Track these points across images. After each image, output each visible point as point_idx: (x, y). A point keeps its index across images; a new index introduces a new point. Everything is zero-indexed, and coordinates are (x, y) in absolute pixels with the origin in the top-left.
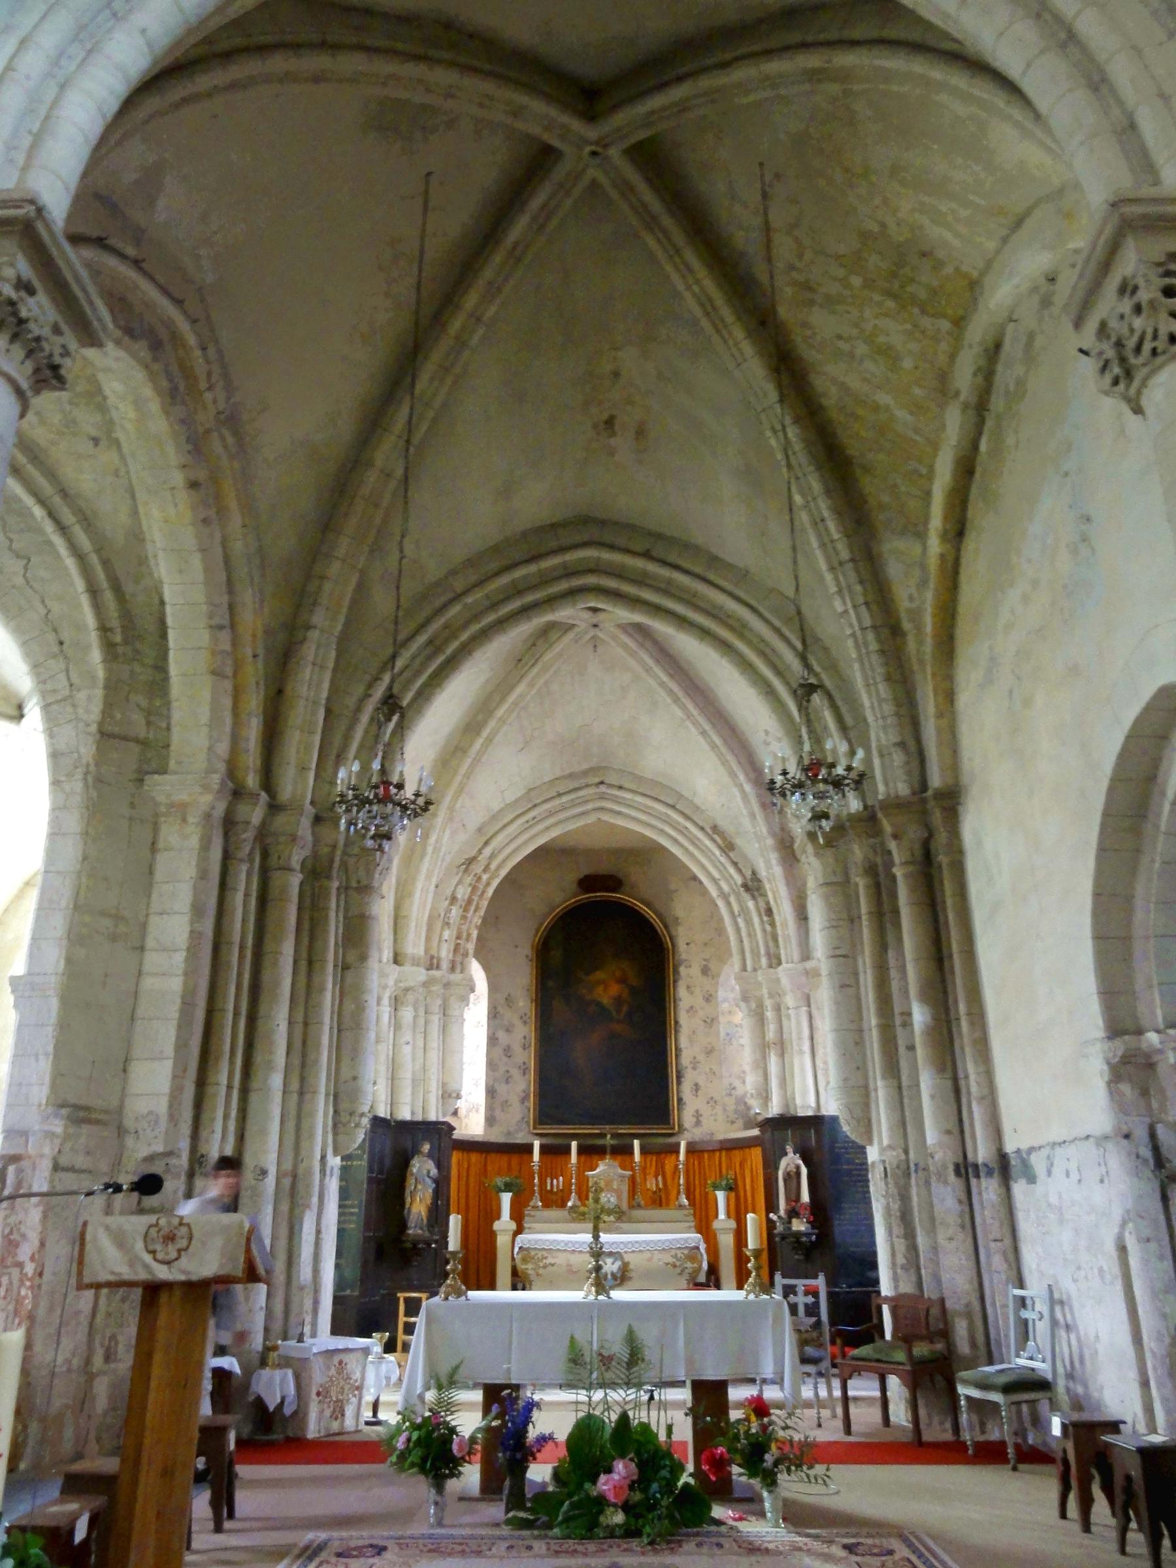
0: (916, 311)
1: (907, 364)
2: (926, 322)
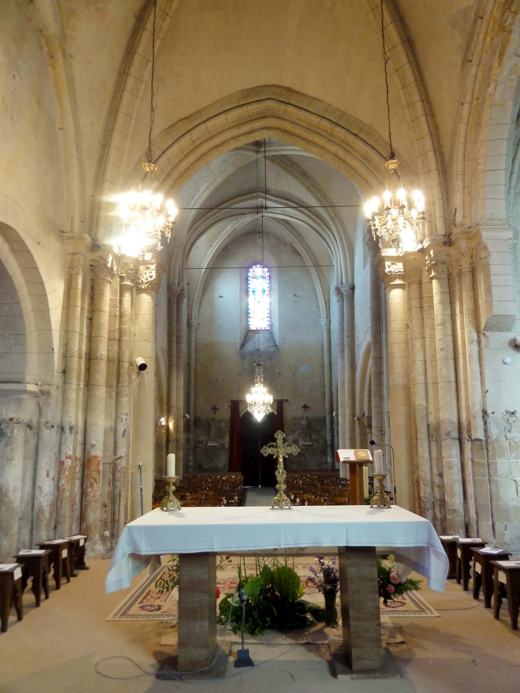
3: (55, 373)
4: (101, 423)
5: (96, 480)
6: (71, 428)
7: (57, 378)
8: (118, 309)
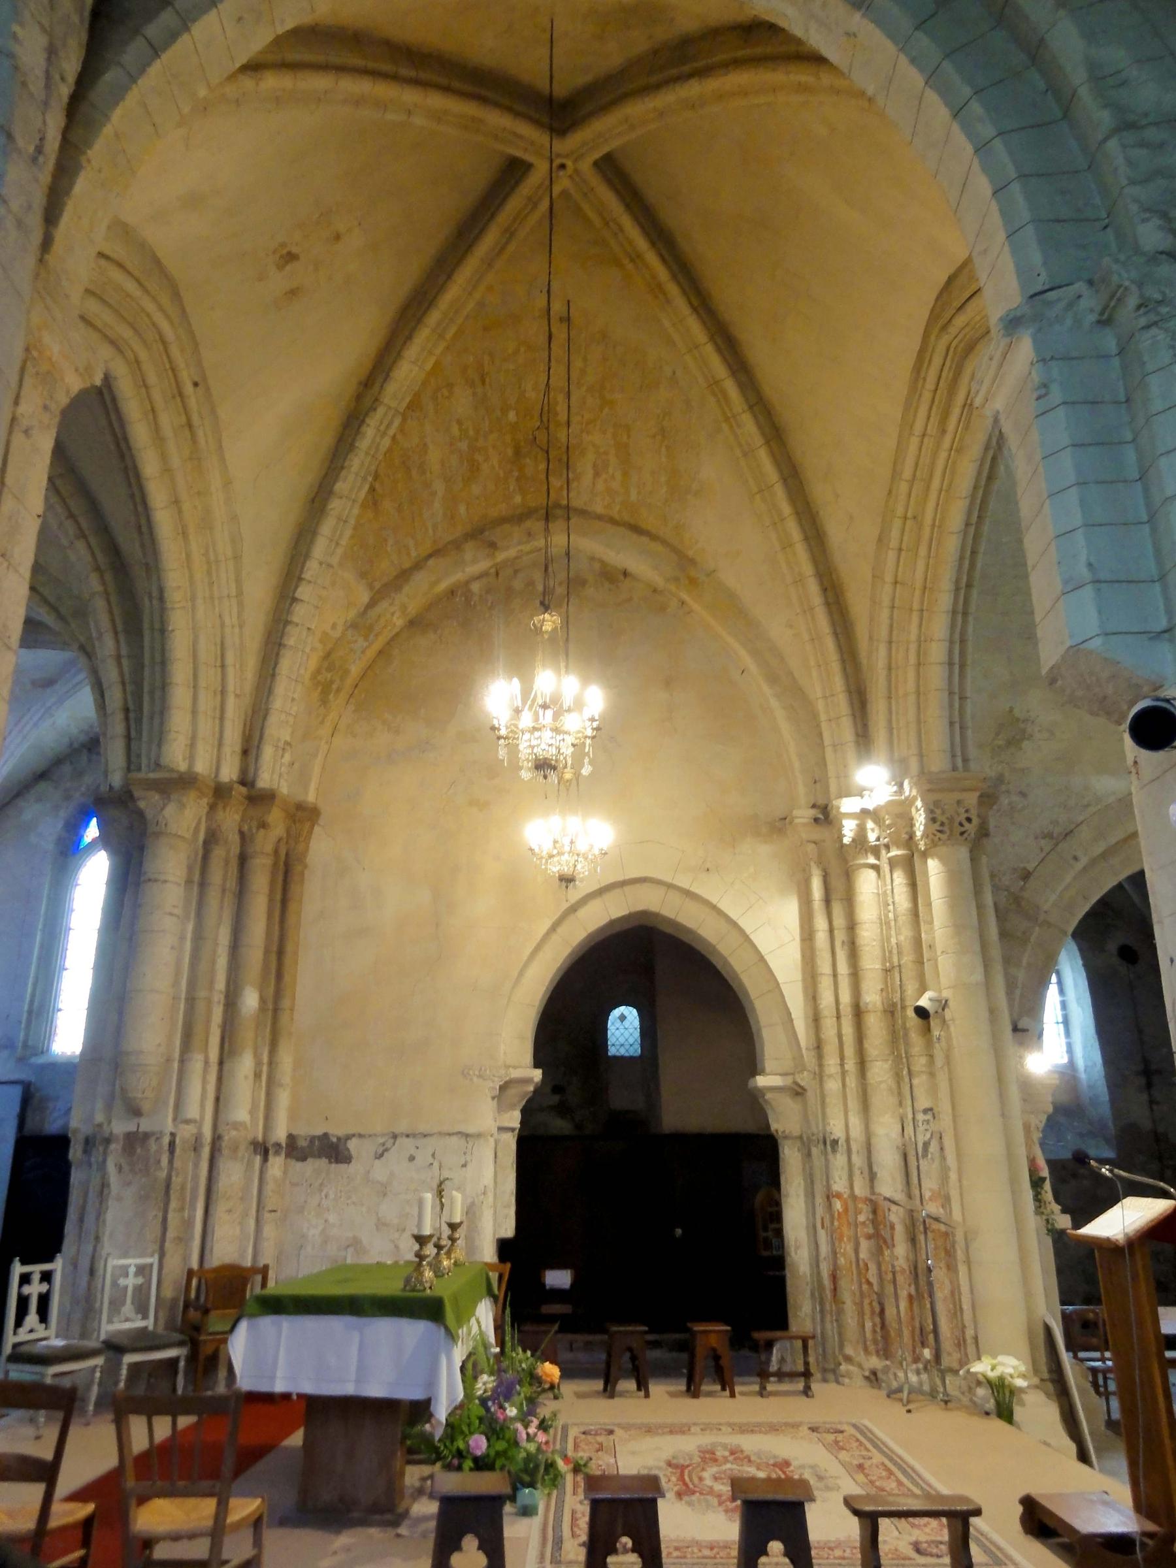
0: (516, 474)
1: (476, 489)
2: (512, 486)
3: (804, 1051)
4: (887, 1131)
5: (885, 1242)
6: (835, 1142)
7: (809, 1057)
8: (891, 907)
